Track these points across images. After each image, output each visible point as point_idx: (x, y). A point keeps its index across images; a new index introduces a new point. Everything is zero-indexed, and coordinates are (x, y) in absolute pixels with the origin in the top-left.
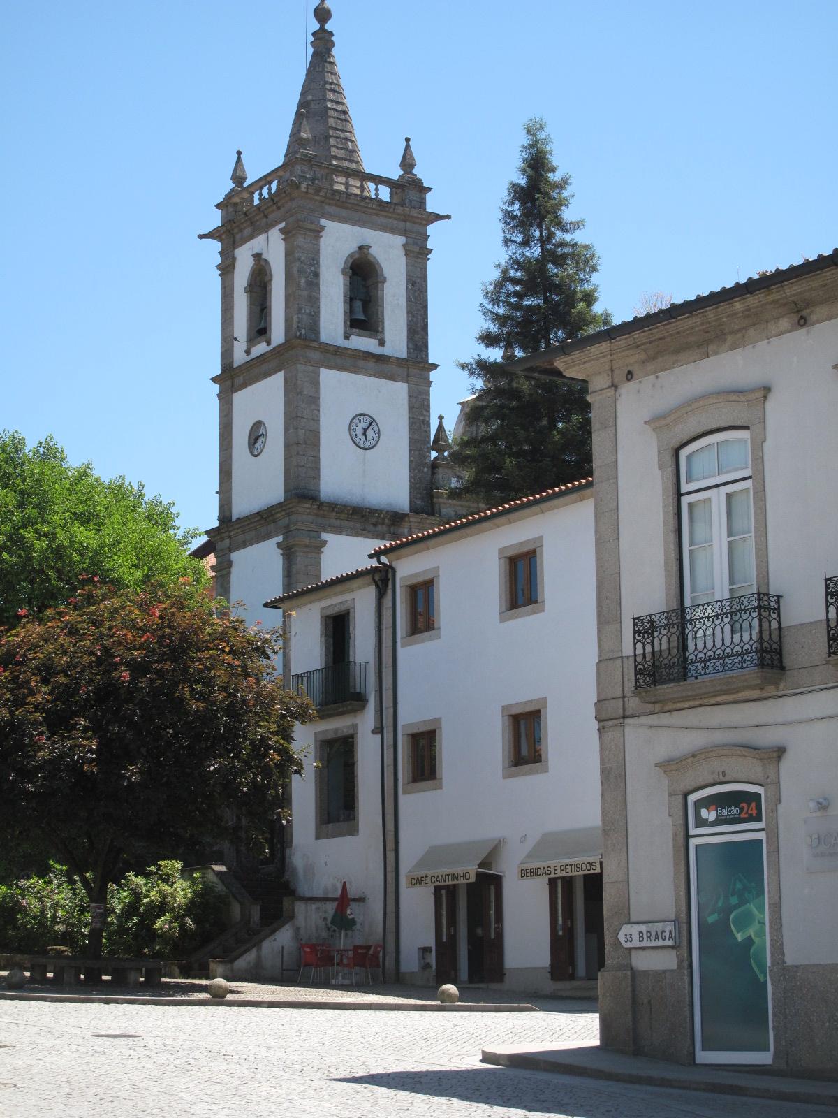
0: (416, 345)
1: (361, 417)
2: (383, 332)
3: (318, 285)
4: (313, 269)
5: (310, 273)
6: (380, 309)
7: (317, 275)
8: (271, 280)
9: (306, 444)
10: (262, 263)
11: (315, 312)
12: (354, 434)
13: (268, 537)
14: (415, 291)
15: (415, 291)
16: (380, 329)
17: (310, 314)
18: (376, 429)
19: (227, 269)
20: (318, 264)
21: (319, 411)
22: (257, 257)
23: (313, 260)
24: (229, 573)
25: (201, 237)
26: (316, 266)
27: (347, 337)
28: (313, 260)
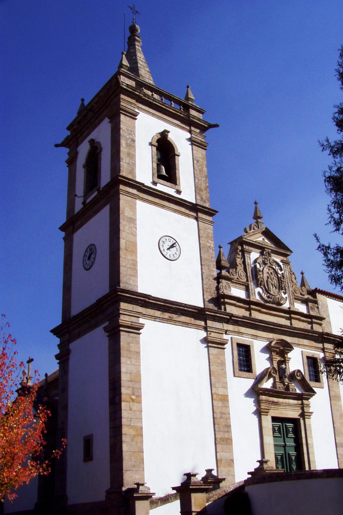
0: (202, 198)
1: (167, 238)
2: (179, 185)
3: (134, 147)
4: (131, 136)
5: (129, 139)
6: (177, 171)
7: (134, 141)
8: (101, 151)
9: (126, 250)
10: (95, 145)
11: (133, 163)
12: (162, 249)
13: (96, 325)
14: (199, 166)
15: (199, 166)
16: (178, 183)
17: (129, 164)
18: (178, 247)
19: (71, 162)
20: (134, 134)
21: (136, 228)
22: (92, 142)
23: (131, 132)
24: (68, 359)
25: (57, 146)
26: (133, 135)
27: (155, 183)
28: (131, 132)
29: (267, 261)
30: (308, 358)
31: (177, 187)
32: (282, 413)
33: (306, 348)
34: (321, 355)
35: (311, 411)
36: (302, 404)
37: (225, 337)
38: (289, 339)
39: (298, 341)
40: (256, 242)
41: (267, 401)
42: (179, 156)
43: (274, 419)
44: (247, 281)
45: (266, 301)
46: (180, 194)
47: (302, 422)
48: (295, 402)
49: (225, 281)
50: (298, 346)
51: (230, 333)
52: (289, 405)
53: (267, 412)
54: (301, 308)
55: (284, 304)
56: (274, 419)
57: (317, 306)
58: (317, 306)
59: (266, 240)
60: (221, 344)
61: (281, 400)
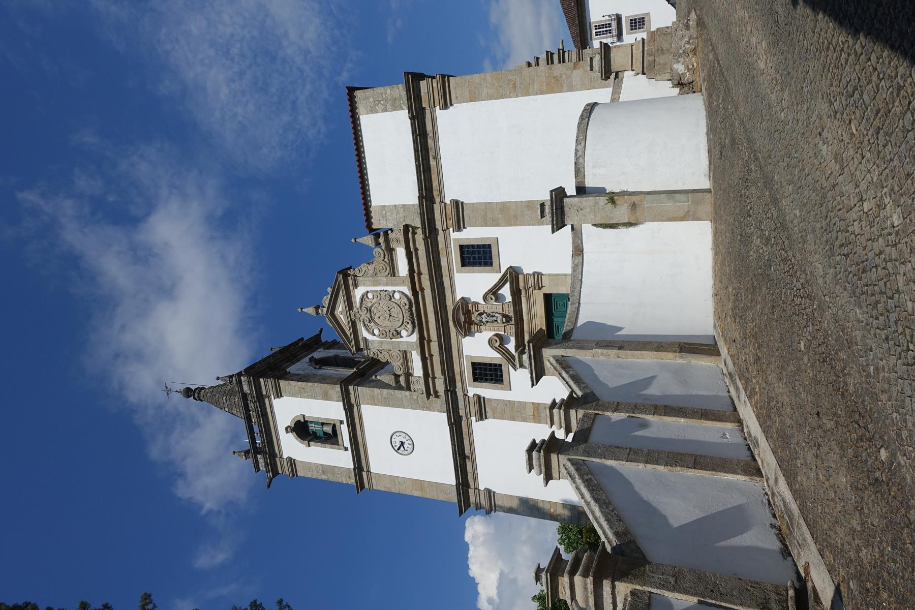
29: (365, 321)
30: (463, 265)
31: (338, 424)
33: (451, 264)
37: (470, 394)
38: (450, 307)
42: (304, 416)
45: (414, 327)
46: (343, 421)
48: (523, 300)
49: (411, 385)
50: (453, 278)
52: (530, 312)
57: (390, 232)
59: (340, 309)
60: (480, 401)
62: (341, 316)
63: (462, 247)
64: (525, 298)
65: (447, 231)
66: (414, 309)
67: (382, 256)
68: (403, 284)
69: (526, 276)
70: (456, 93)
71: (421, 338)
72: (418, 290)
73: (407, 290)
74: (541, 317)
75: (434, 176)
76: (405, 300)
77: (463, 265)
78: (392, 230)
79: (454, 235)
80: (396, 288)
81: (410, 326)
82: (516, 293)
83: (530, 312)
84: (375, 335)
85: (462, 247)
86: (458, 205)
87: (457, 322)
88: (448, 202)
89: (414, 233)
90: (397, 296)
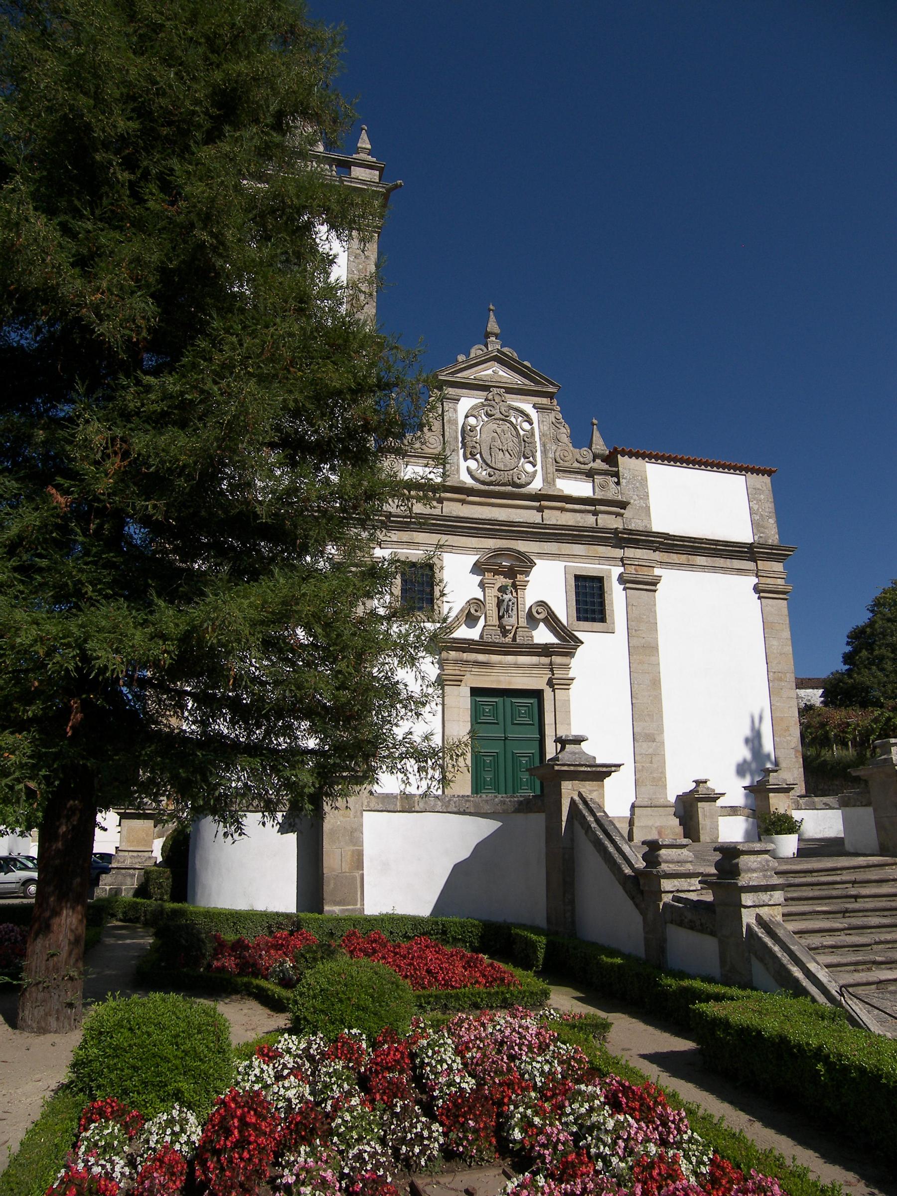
30: (578, 578)
32: (499, 682)
34: (617, 571)
35: (571, 675)
36: (551, 664)
39: (559, 549)
40: (475, 379)
41: (456, 662)
43: (475, 692)
44: (444, 449)
45: (483, 483)
47: (548, 695)
48: (535, 659)
51: (389, 546)
52: (517, 666)
53: (461, 681)
54: (581, 488)
55: (529, 484)
56: (475, 692)
57: (616, 480)
58: (616, 480)
59: (501, 373)
61: (495, 658)
62: (490, 372)
63: (600, 580)
64: (537, 663)
65: (621, 564)
66: (509, 488)
67: (581, 460)
68: (545, 480)
69: (567, 667)
70: (772, 606)
71: (470, 492)
72: (542, 503)
73: (537, 485)
74: (510, 683)
75: (683, 558)
76: (524, 479)
77: (578, 578)
78: (618, 483)
79: (617, 571)
80: (539, 467)
81: (483, 474)
82: (545, 650)
83: (517, 666)
84: (467, 417)
85: (600, 580)
86: (652, 584)
87: (499, 553)
88: (657, 571)
89: (617, 515)
90: (529, 468)
